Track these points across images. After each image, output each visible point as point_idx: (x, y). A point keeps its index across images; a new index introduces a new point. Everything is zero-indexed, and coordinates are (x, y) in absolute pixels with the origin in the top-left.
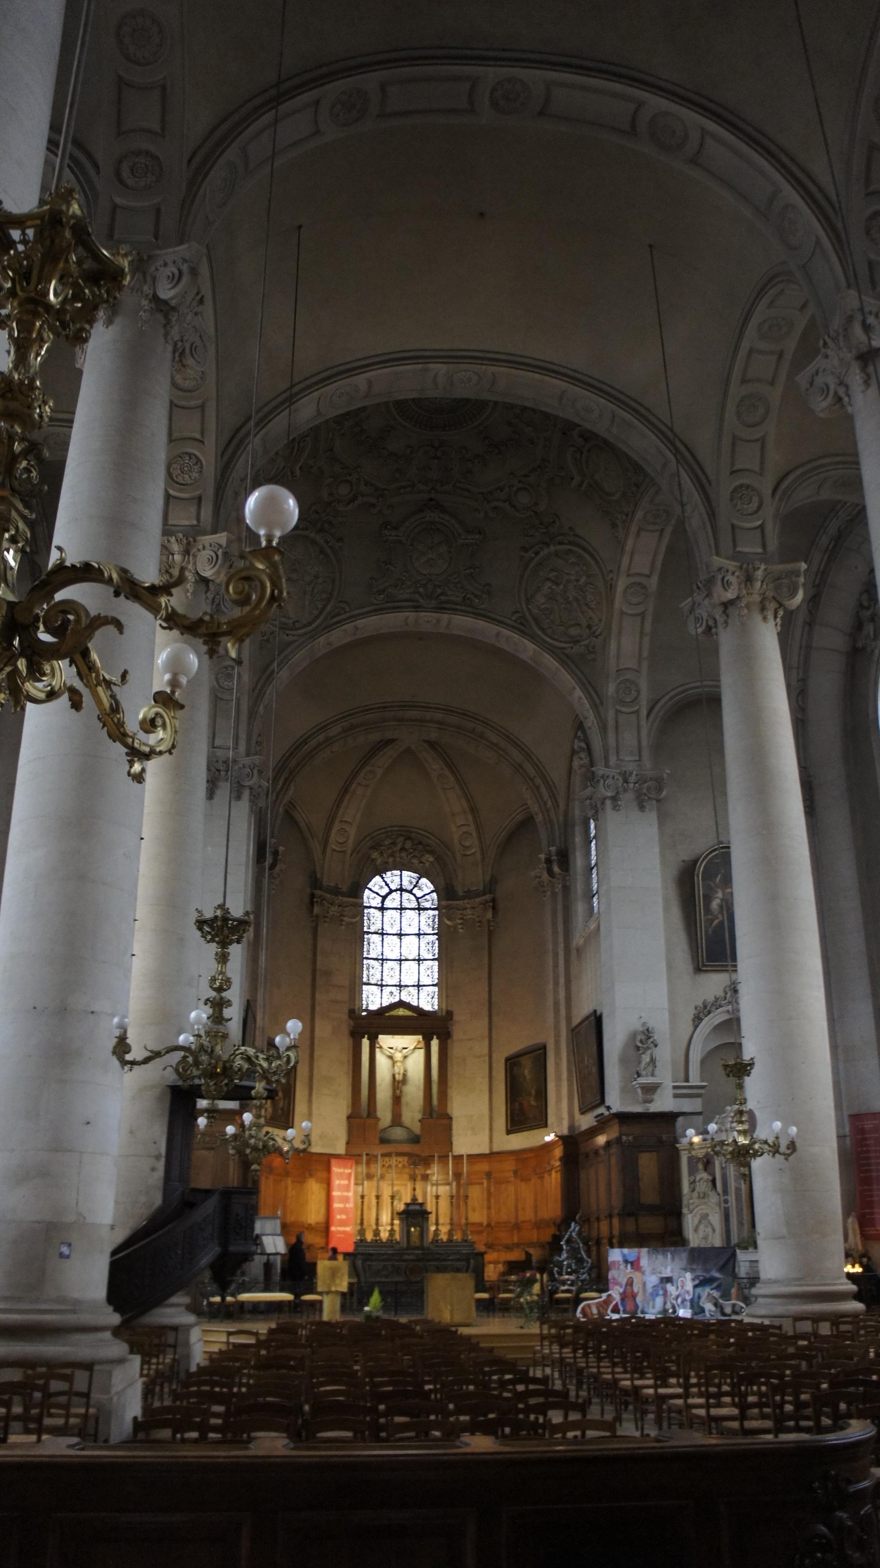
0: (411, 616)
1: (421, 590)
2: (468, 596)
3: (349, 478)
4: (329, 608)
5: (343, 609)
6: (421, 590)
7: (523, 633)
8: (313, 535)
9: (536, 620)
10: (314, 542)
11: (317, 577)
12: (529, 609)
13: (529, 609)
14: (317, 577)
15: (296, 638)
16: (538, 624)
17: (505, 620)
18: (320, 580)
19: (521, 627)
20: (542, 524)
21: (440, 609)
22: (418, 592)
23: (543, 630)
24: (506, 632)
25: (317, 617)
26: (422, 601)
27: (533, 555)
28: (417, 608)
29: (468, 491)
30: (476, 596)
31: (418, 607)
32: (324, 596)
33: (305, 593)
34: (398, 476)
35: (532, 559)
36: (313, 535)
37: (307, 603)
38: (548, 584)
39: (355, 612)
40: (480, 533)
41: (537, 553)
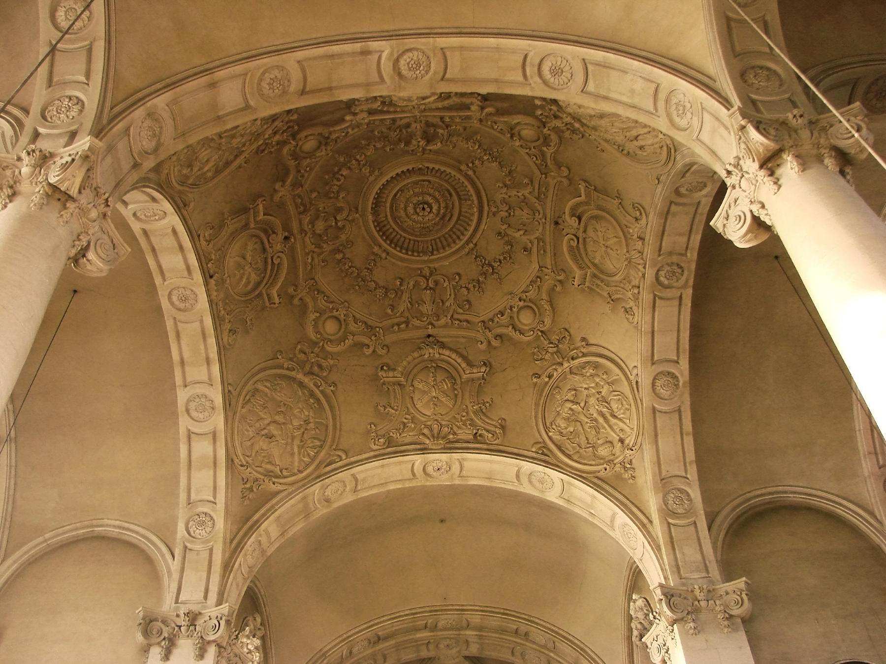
0: (418, 460)
1: (426, 431)
2: (480, 432)
3: (335, 313)
4: (322, 454)
5: (340, 456)
6: (426, 431)
7: (547, 464)
8: (300, 376)
9: (559, 448)
10: (301, 384)
11: (307, 422)
12: (550, 438)
13: (550, 438)
14: (307, 422)
15: (285, 487)
16: (563, 452)
17: (526, 453)
18: (312, 425)
19: (544, 457)
20: (552, 343)
21: (450, 447)
22: (423, 434)
23: (569, 456)
24: (527, 466)
25: (308, 465)
26: (427, 442)
27: (547, 379)
28: (424, 450)
29: (468, 321)
30: (488, 431)
31: (426, 449)
32: (318, 443)
33: (293, 438)
34: (389, 311)
35: (547, 383)
36: (300, 376)
37: (296, 450)
38: (569, 405)
39: (353, 459)
40: (485, 364)
41: (550, 377)
